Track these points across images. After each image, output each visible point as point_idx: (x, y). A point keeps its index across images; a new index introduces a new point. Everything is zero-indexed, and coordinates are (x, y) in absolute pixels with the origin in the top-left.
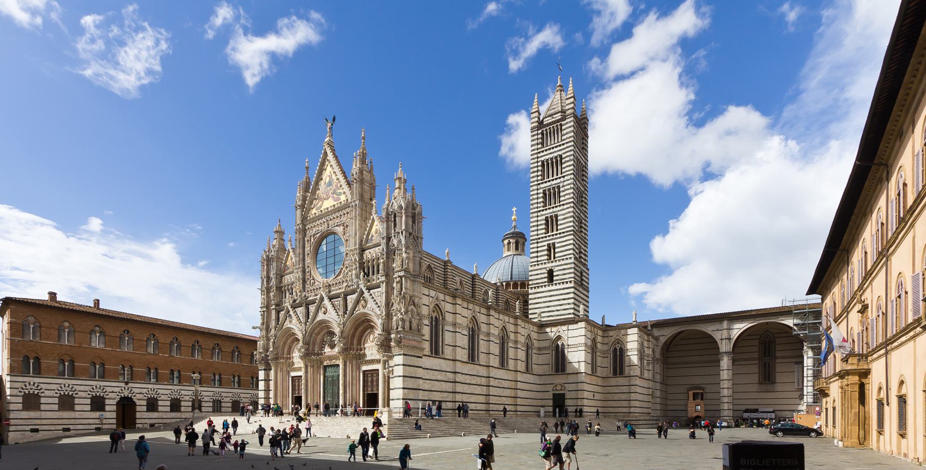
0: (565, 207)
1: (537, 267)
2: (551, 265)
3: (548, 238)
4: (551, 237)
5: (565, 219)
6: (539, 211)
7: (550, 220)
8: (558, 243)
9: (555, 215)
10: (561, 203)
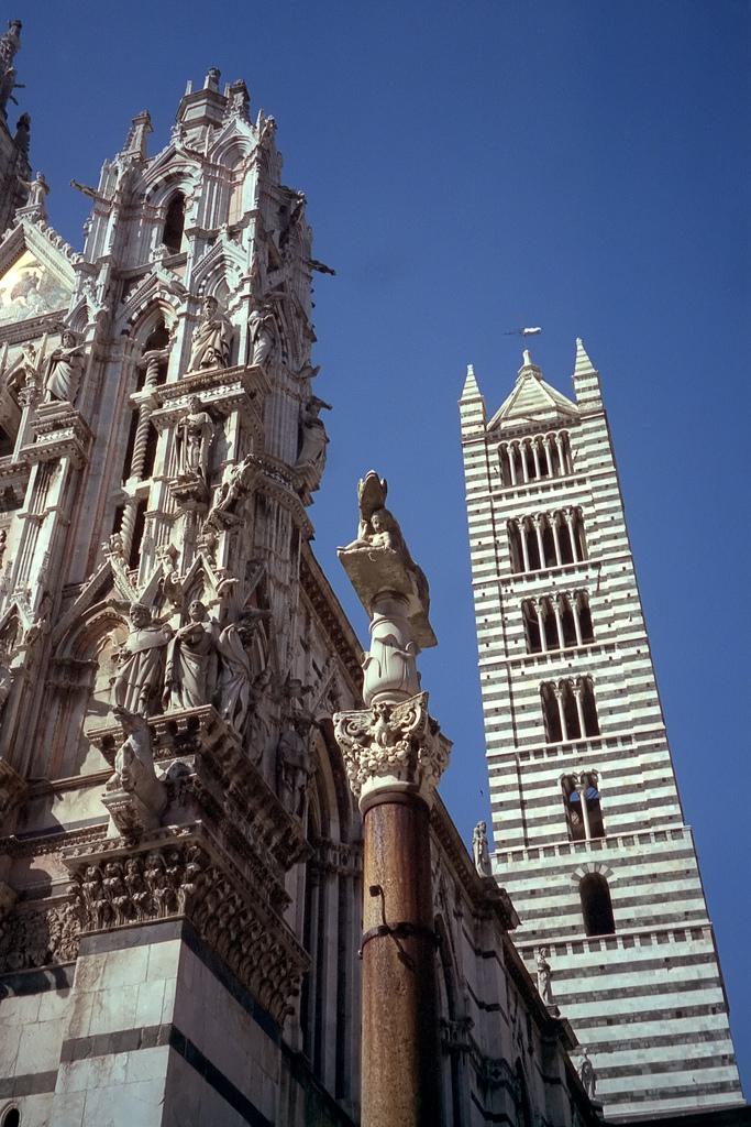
0: (618, 654)
1: (526, 864)
2: (585, 858)
3: (561, 757)
4: (575, 754)
5: (622, 693)
6: (516, 664)
7: (559, 695)
8: (607, 775)
9: (579, 678)
10: (600, 643)
